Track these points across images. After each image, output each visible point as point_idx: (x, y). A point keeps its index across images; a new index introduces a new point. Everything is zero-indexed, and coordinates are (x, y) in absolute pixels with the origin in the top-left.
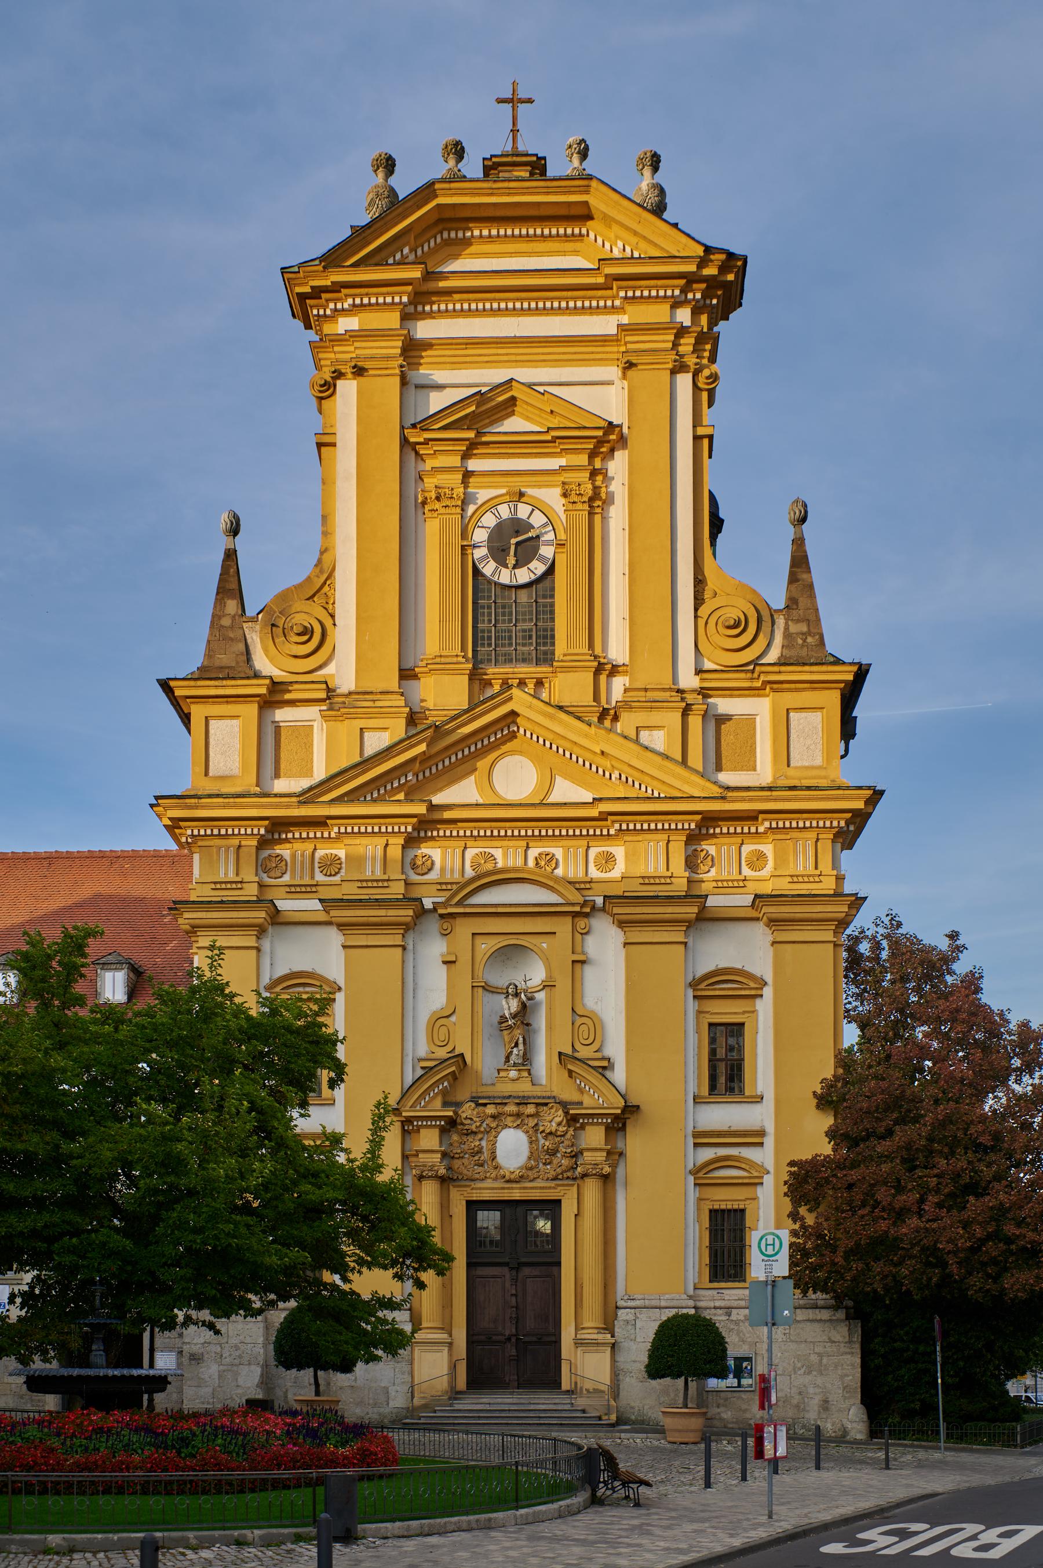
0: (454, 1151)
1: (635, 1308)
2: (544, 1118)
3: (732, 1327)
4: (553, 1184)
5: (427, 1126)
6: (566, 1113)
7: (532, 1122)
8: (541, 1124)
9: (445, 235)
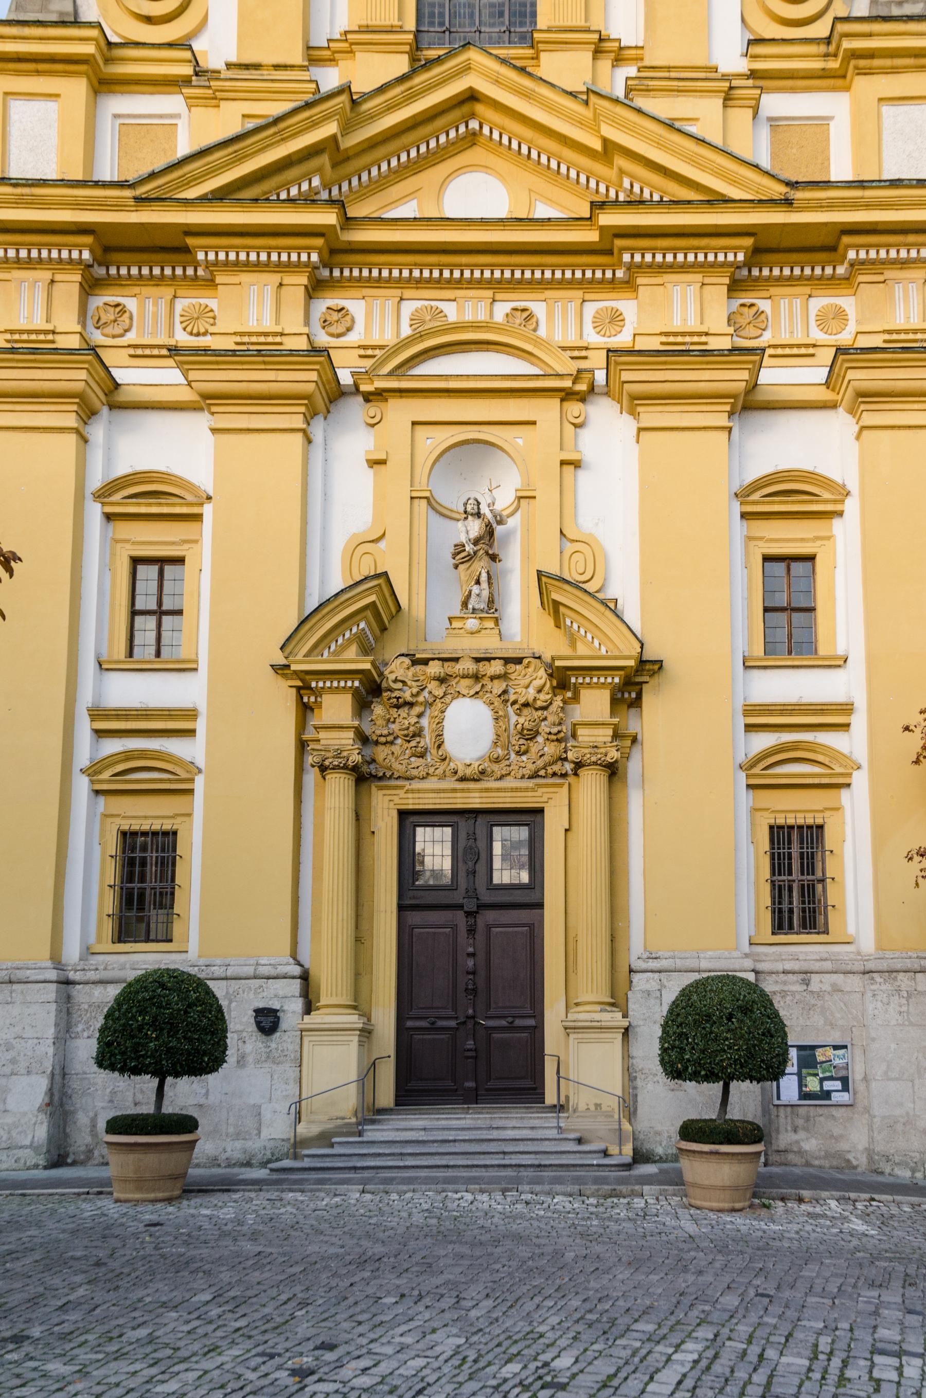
0: (378, 732)
1: (660, 972)
2: (516, 682)
3: (813, 1002)
4: (531, 783)
8: (512, 691)
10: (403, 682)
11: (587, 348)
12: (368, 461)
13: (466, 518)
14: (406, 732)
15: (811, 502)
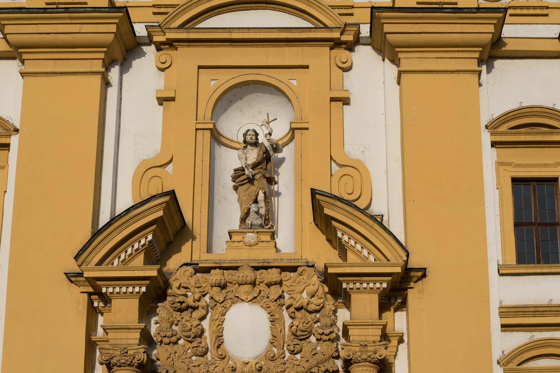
7: (275, 292)
8: (287, 296)
10: (186, 288)
11: (353, 7)
12: (158, 99)
13: (245, 147)
14: (188, 334)
15: (552, 133)
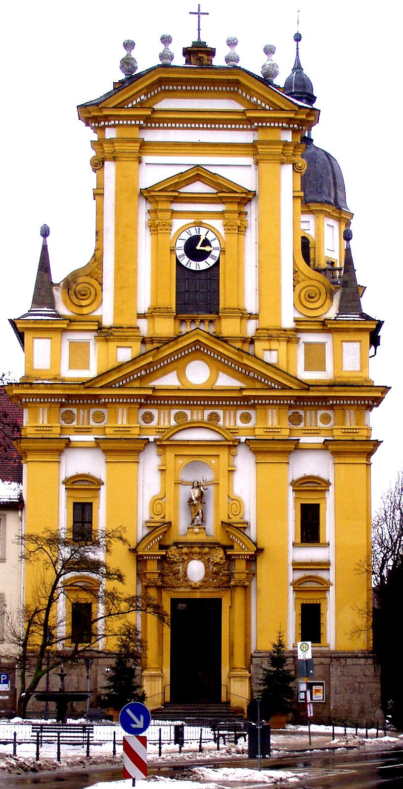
4: (217, 590)
5: (151, 559)
6: (225, 552)
9: (163, 87)
